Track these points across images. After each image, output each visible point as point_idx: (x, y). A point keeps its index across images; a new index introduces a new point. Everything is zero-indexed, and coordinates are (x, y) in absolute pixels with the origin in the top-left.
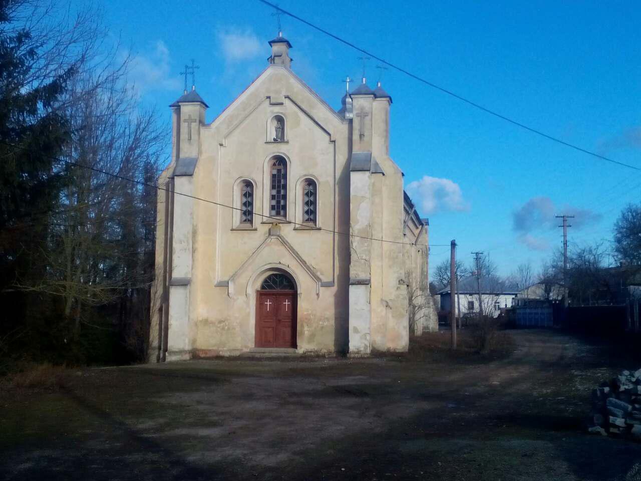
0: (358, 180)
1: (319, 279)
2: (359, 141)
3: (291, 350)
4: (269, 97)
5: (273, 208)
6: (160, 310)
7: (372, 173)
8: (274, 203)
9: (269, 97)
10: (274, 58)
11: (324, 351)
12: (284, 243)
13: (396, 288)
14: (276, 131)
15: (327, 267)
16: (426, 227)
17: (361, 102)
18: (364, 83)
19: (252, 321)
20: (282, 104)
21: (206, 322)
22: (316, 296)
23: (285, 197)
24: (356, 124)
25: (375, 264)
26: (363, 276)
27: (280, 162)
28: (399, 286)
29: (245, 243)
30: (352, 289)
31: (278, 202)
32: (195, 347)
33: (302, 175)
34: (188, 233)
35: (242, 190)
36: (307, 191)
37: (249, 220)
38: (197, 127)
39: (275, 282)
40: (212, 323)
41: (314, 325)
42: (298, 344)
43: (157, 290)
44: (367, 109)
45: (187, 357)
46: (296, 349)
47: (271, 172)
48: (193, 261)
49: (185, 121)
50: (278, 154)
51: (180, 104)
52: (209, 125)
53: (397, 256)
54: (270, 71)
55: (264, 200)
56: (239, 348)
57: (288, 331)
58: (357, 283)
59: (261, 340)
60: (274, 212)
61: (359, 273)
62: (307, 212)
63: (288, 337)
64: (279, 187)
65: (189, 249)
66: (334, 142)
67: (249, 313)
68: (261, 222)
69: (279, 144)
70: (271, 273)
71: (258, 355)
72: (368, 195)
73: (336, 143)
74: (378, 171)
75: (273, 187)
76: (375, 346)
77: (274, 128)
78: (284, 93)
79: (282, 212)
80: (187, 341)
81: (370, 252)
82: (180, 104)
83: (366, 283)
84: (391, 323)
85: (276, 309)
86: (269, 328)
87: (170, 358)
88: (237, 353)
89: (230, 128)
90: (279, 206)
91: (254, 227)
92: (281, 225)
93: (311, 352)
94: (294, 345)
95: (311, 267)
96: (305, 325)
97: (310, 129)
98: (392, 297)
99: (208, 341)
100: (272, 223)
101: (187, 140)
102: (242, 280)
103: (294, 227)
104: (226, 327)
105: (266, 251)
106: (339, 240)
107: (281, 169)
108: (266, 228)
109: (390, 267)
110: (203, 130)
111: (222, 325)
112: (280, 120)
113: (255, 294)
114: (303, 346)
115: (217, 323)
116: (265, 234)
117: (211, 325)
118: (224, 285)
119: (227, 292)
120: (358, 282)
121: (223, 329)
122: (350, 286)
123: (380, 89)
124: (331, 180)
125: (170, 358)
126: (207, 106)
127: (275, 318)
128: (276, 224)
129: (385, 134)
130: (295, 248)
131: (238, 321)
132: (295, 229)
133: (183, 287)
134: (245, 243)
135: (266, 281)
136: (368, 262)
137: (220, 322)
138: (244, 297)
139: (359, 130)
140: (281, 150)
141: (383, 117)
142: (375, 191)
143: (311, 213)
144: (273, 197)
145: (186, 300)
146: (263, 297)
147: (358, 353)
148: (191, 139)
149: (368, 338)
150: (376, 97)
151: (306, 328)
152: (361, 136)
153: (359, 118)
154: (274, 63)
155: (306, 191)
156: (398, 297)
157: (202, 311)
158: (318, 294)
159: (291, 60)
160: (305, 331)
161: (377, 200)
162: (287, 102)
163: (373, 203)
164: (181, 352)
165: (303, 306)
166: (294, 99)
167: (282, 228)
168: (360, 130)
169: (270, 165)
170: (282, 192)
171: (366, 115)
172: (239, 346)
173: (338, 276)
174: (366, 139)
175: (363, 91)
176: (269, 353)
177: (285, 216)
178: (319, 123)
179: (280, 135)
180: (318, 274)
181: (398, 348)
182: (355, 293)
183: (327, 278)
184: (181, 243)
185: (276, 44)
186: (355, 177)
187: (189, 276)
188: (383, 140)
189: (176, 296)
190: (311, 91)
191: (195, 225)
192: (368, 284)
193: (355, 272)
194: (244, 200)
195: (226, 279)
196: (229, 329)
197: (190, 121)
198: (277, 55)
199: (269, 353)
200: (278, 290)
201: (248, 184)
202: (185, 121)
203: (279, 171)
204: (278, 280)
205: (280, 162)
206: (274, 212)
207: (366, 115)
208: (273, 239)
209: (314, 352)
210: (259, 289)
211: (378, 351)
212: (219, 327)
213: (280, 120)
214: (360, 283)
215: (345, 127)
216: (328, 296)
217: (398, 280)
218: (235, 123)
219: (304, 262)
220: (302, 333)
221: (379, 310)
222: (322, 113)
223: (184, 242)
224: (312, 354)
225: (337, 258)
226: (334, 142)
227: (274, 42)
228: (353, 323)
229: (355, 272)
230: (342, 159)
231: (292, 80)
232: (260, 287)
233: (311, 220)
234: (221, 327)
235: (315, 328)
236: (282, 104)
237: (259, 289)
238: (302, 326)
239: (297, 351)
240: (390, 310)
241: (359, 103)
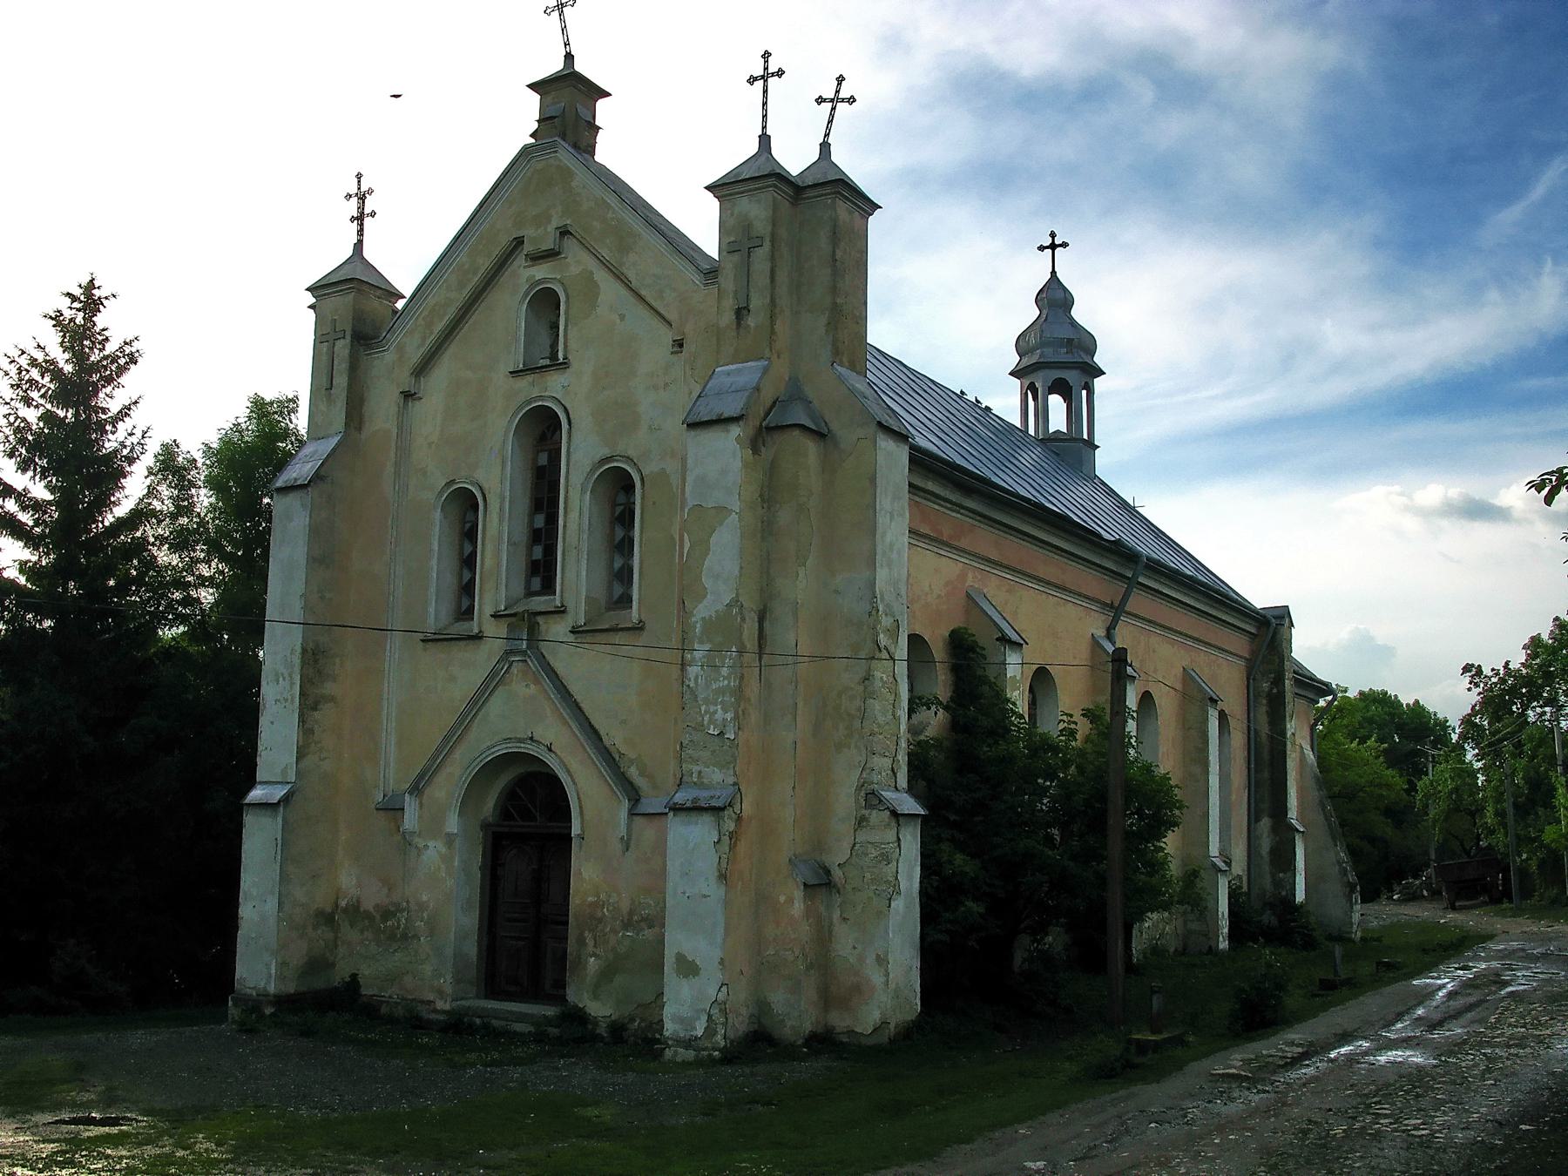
2: (734, 334)
22: (618, 847)
28: (866, 812)
40: (368, 916)
47: (535, 460)
60: (536, 583)
72: (736, 505)
92: (540, 619)
140: (554, 388)
174: (751, 321)
178: (643, 293)
180: (633, 772)
217: (863, 794)
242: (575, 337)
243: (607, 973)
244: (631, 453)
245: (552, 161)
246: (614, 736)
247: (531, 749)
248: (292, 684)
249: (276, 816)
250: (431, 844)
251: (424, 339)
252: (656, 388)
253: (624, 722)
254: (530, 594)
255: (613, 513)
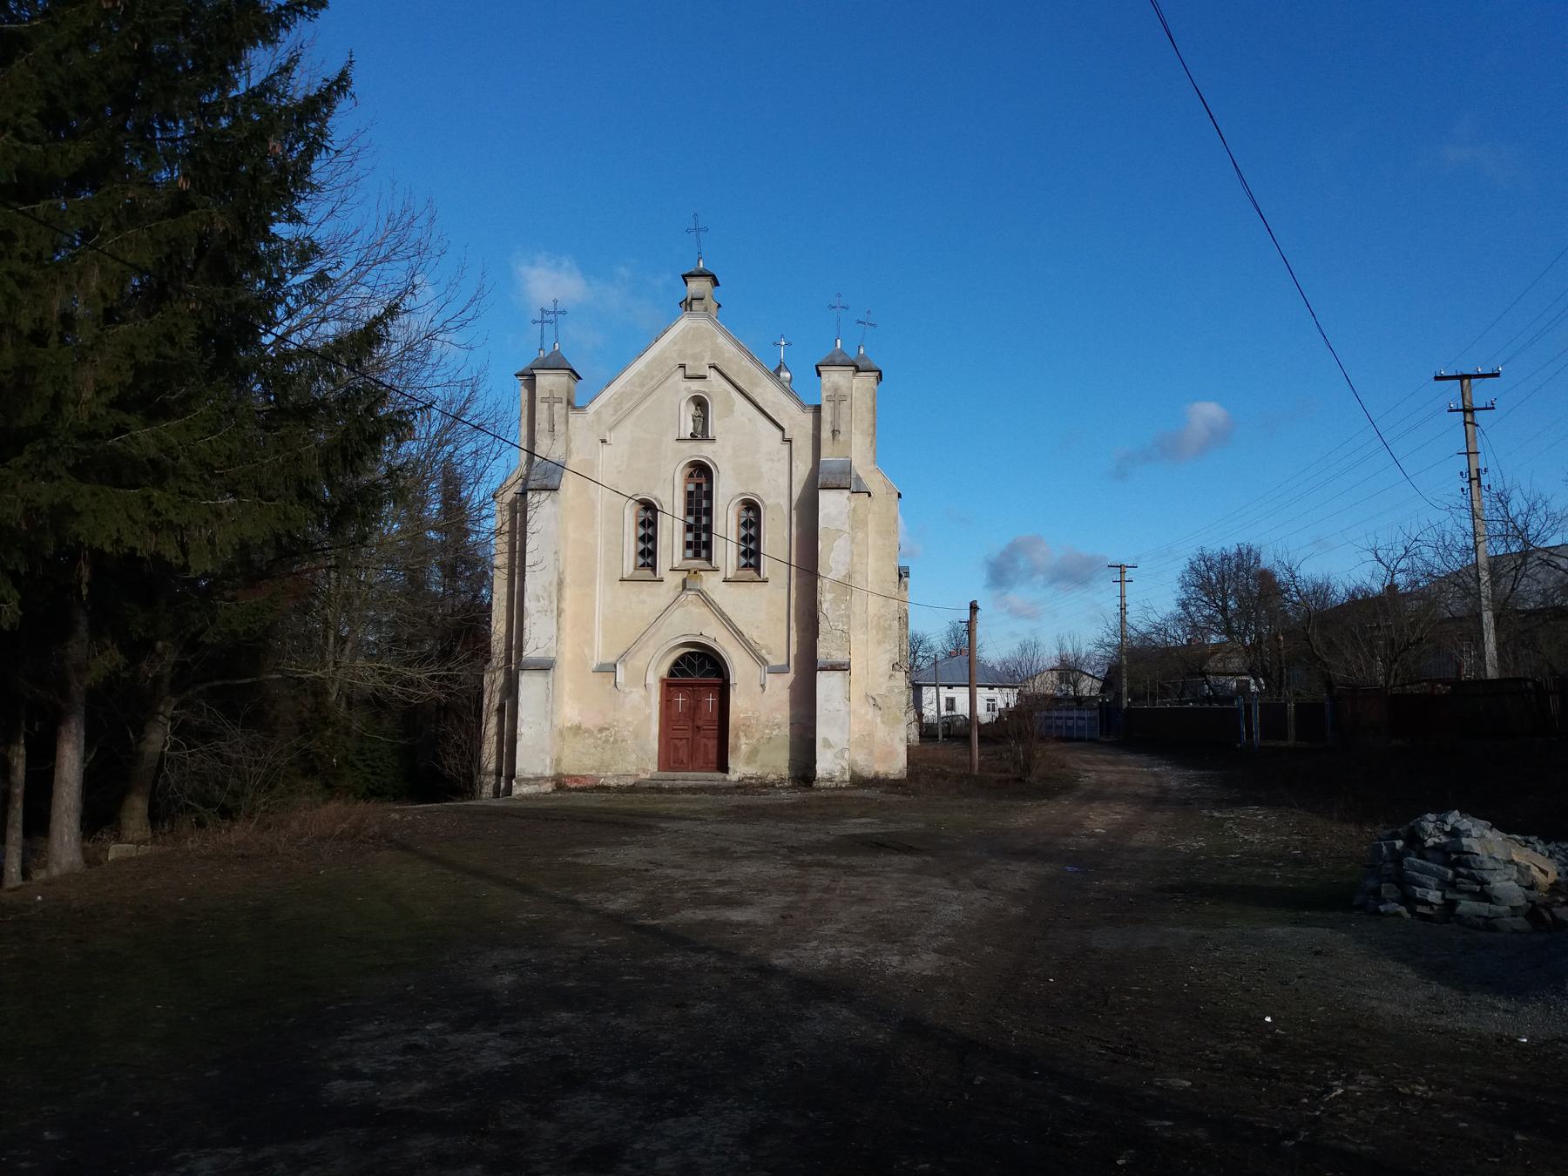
0: (831, 503)
1: (764, 661)
3: (719, 775)
4: (683, 366)
5: (688, 545)
6: (501, 710)
7: (853, 492)
8: (690, 537)
9: (683, 366)
10: (691, 302)
11: (772, 777)
12: (708, 602)
13: (887, 677)
14: (694, 421)
15: (777, 639)
16: (906, 579)
17: (834, 378)
18: (839, 346)
19: (655, 729)
20: (704, 377)
21: (577, 730)
23: (708, 528)
24: (826, 414)
25: (857, 637)
26: (838, 657)
27: (701, 472)
29: (644, 602)
30: (821, 677)
31: (698, 537)
32: (559, 771)
33: (737, 493)
34: (550, 584)
35: (637, 516)
36: (745, 519)
37: (649, 565)
38: (564, 412)
39: (691, 665)
40: (587, 731)
41: (757, 736)
42: (731, 765)
43: (494, 680)
44: (844, 390)
45: (548, 787)
46: (724, 774)
47: (685, 487)
48: (559, 629)
49: (543, 400)
50: (697, 459)
51: (535, 372)
52: (583, 408)
53: (890, 625)
54: (684, 323)
55: (675, 533)
56: (634, 772)
57: (712, 744)
58: (829, 668)
59: (670, 757)
60: (690, 553)
61: (833, 653)
62: (744, 554)
63: (713, 756)
64: (698, 512)
65: (552, 611)
66: (790, 441)
67: (649, 717)
68: (670, 567)
69: (698, 443)
70: (687, 650)
71: (666, 785)
72: (846, 528)
73: (793, 445)
74: (862, 491)
75: (689, 512)
76: (856, 769)
77: (691, 418)
78: (708, 360)
79: (704, 553)
80: (548, 761)
81: (848, 617)
82: (535, 372)
83: (843, 667)
84: (881, 732)
85: (694, 709)
86: (681, 739)
87: (519, 790)
88: (630, 781)
89: (620, 413)
90: (700, 543)
91: (658, 576)
92: (702, 573)
93: (751, 778)
94: (723, 767)
95: (751, 641)
96: (741, 734)
97: (750, 420)
98: (883, 691)
99: (582, 762)
100: (689, 570)
101: (546, 432)
102: (639, 661)
103: (724, 576)
104: (612, 739)
105: (677, 615)
106: (797, 597)
107: (701, 484)
108: (680, 576)
109: (879, 643)
110: (574, 417)
111: (604, 734)
112: (700, 403)
113: (659, 685)
114: (739, 769)
115: (596, 732)
116: (677, 587)
117: (586, 734)
118: (608, 669)
119: (613, 683)
120: (831, 666)
121: (607, 741)
122: (818, 672)
123: (864, 357)
124: (784, 502)
125: (519, 790)
126: (579, 378)
127: (690, 724)
128: (695, 573)
129: (871, 430)
130: (725, 610)
131: (631, 729)
132: (726, 580)
133: (542, 673)
134: (644, 602)
135: (676, 664)
136: (846, 636)
137: (601, 730)
138: (642, 691)
139: (831, 422)
140: (703, 451)
141: (870, 403)
142: (857, 522)
143: (751, 554)
144: (689, 528)
145: (548, 695)
146: (671, 689)
147: (830, 780)
148: (553, 431)
149: (846, 756)
150: (858, 370)
151: (743, 740)
152: (835, 432)
153: (832, 404)
154: (691, 310)
155: (743, 520)
156: (891, 690)
157: (570, 712)
158: (763, 686)
159: (719, 306)
160: (741, 745)
161: (860, 535)
162: (712, 374)
163: (853, 540)
164: (538, 779)
165: (739, 704)
166: (725, 371)
167: (704, 578)
168: (833, 423)
169: (684, 475)
170: (704, 520)
171: (843, 399)
172: (633, 769)
173: (796, 656)
174: (841, 437)
175: (838, 360)
176: (683, 780)
177: (709, 559)
179: (700, 428)
180: (763, 652)
181: (891, 772)
182: (826, 684)
183: (777, 660)
184: (539, 601)
185: (694, 279)
186: (825, 498)
187: (553, 655)
188: (868, 440)
189: (530, 687)
190: (752, 358)
191: (561, 571)
192: (847, 670)
193: (825, 651)
194: (641, 532)
195: (612, 660)
196: (616, 741)
197: (551, 400)
198: (695, 297)
199: (683, 780)
200: (696, 678)
201: (648, 506)
202: (543, 400)
203: (699, 486)
204: (696, 663)
205: (701, 472)
206: (690, 553)
207: (843, 399)
208: (691, 595)
209: (757, 779)
210: (666, 677)
211: (862, 777)
212: (600, 739)
213: (700, 403)
214: (834, 668)
215: (807, 419)
216: (780, 688)
218: (626, 406)
219: (740, 634)
220: (737, 748)
221: (863, 712)
222: (769, 393)
223: (544, 599)
224: (753, 781)
225: (795, 629)
226: (790, 441)
227: (691, 275)
228: (822, 732)
229: (826, 650)
230: (803, 468)
231: (721, 340)
232: (666, 672)
233: (751, 566)
234: (603, 739)
235: (758, 740)
236: (704, 377)
237: (666, 677)
238: (737, 736)
239: (728, 777)
240: (881, 712)
241: (832, 379)
242: (715, 425)
243: (754, 752)
244: (757, 492)
245: (701, 324)
246: (751, 633)
247: (703, 640)
248: (551, 602)
249: (547, 676)
250: (634, 690)
251: (616, 411)
252: (772, 460)
253: (758, 627)
254: (687, 559)
255: (739, 521)
